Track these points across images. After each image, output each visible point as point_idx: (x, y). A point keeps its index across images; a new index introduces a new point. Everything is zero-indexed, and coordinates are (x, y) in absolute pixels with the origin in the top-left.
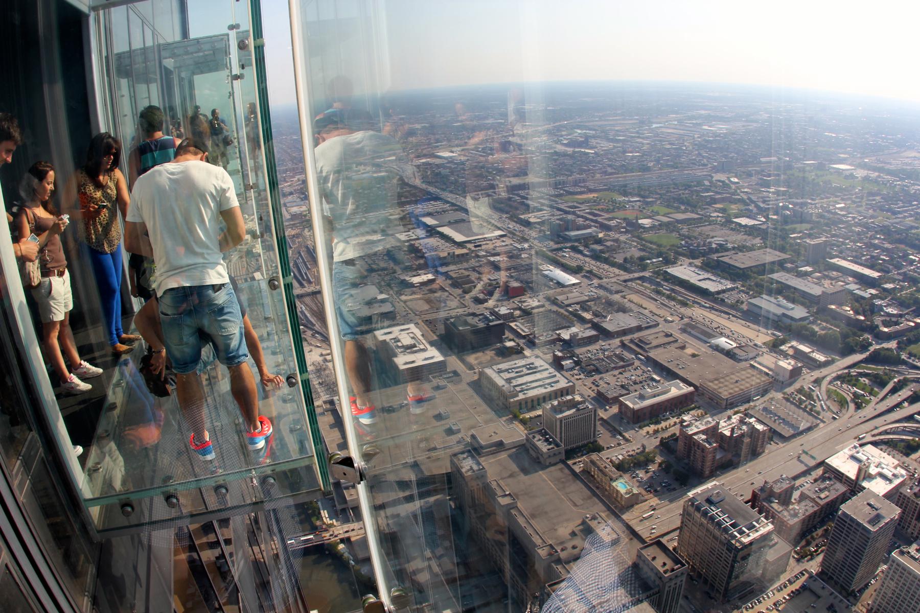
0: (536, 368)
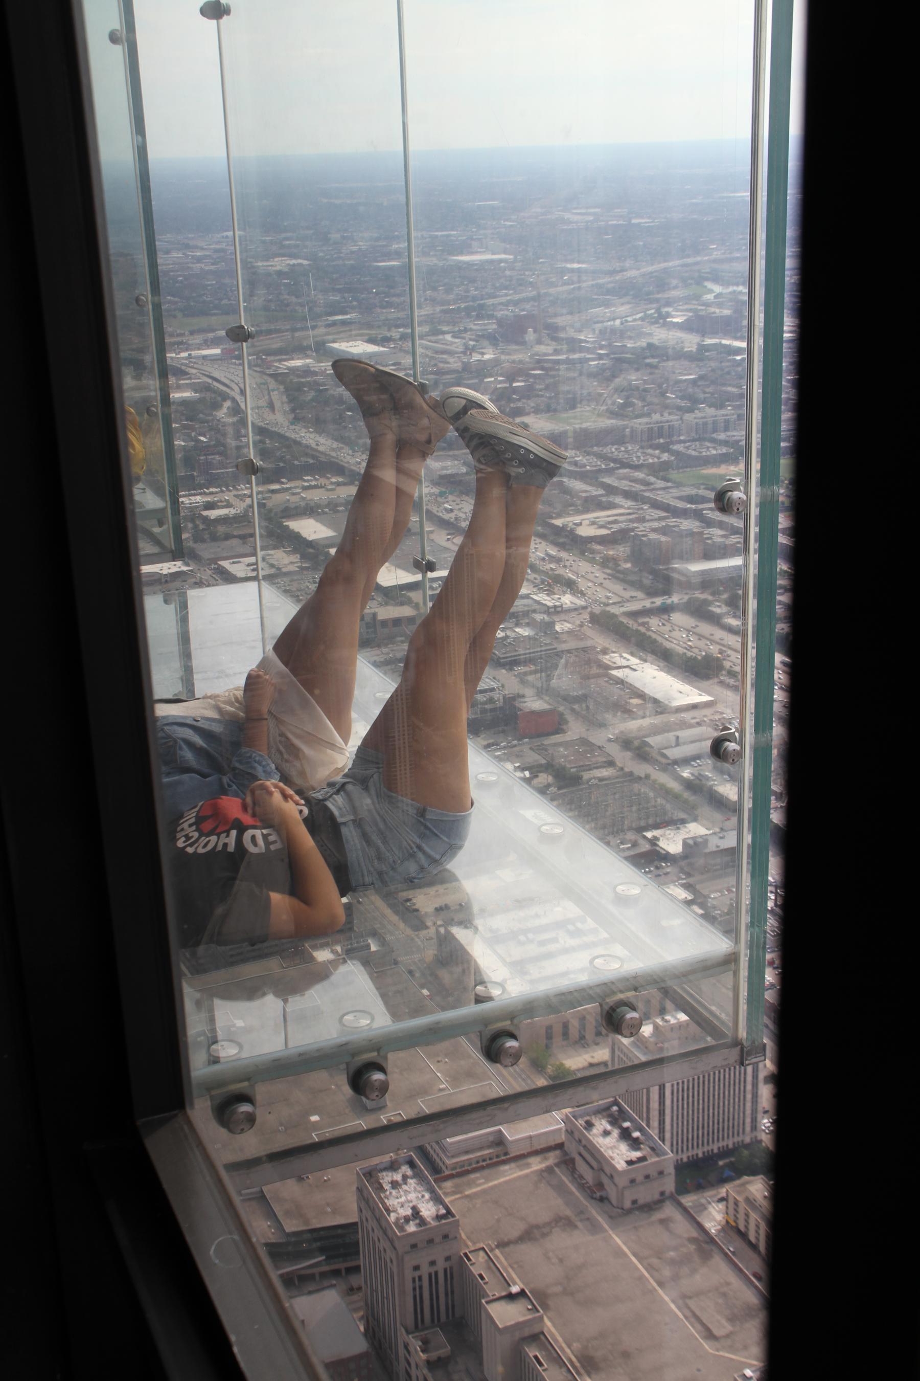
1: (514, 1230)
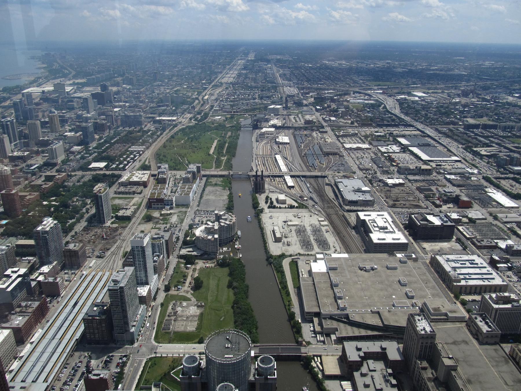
0: (477, 264)
1: (450, 341)
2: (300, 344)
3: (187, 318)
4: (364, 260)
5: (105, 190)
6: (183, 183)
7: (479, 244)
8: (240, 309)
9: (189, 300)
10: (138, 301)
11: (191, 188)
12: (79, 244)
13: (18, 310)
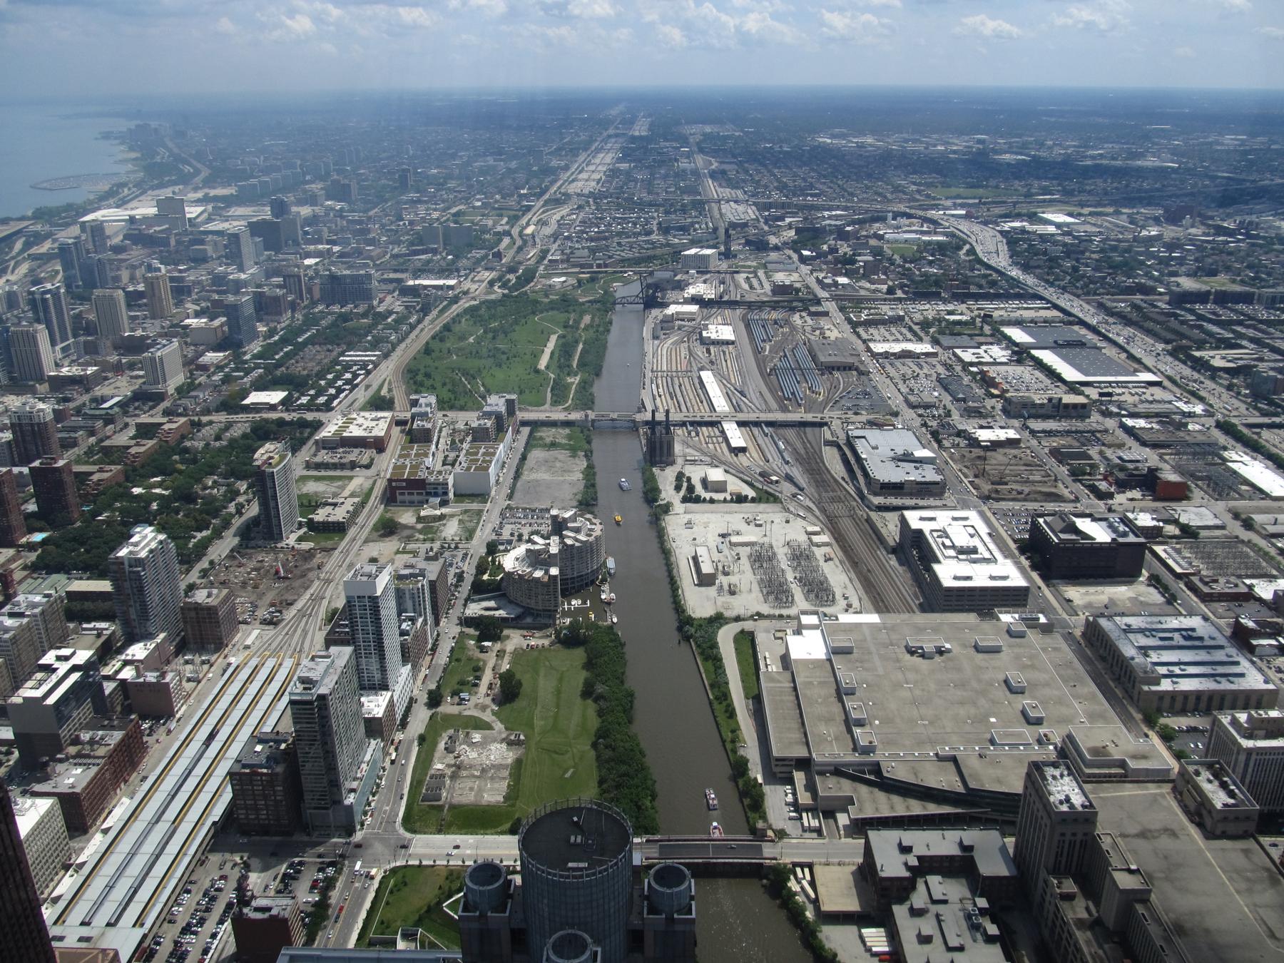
0: (1201, 639)
1: (1133, 829)
2: (759, 835)
3: (483, 771)
4: (920, 630)
5: (282, 458)
6: (474, 440)
7: (1206, 590)
8: (614, 750)
9: (488, 726)
10: (362, 729)
11: (494, 454)
12: (220, 591)
13: (72, 750)
